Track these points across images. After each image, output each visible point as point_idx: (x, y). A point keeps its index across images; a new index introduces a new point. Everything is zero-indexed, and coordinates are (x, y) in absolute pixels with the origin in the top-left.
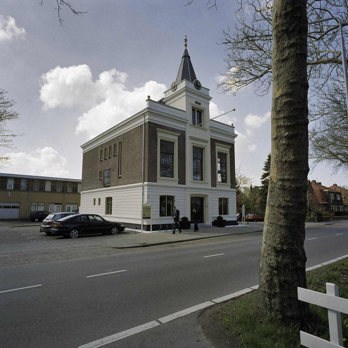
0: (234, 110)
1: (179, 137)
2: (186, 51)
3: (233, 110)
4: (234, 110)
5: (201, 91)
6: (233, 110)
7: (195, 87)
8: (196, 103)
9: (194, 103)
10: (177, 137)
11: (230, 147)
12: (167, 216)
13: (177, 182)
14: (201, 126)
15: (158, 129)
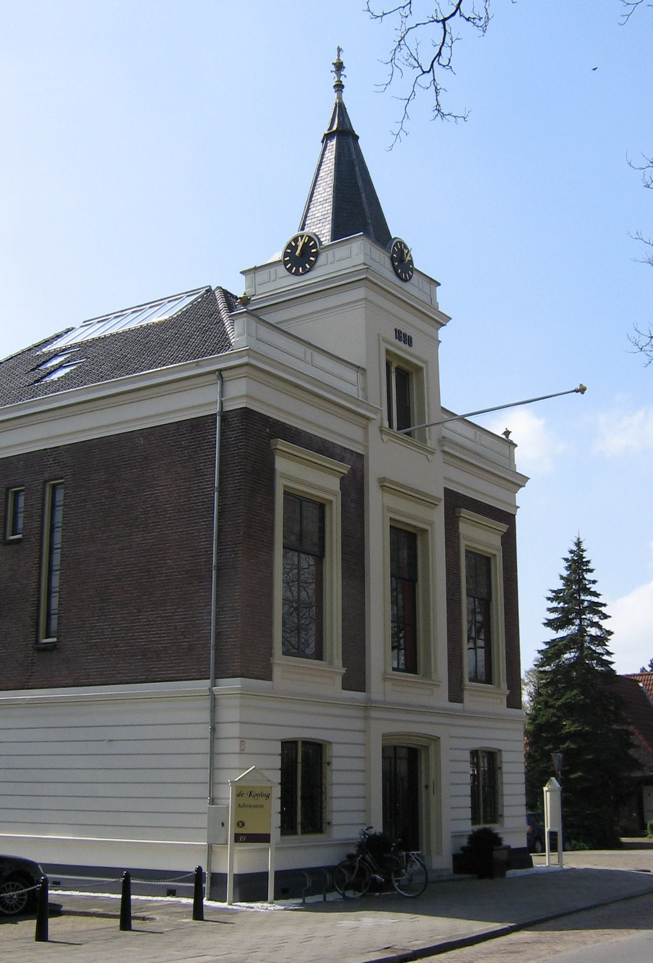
0: (582, 390)
1: (342, 480)
2: (341, 110)
3: (576, 391)
4: (582, 390)
5: (412, 288)
6: (576, 391)
7: (395, 269)
8: (399, 335)
9: (392, 336)
10: (338, 482)
11: (344, 468)
12: (302, 833)
13: (339, 681)
14: (408, 434)
15: (281, 444)
